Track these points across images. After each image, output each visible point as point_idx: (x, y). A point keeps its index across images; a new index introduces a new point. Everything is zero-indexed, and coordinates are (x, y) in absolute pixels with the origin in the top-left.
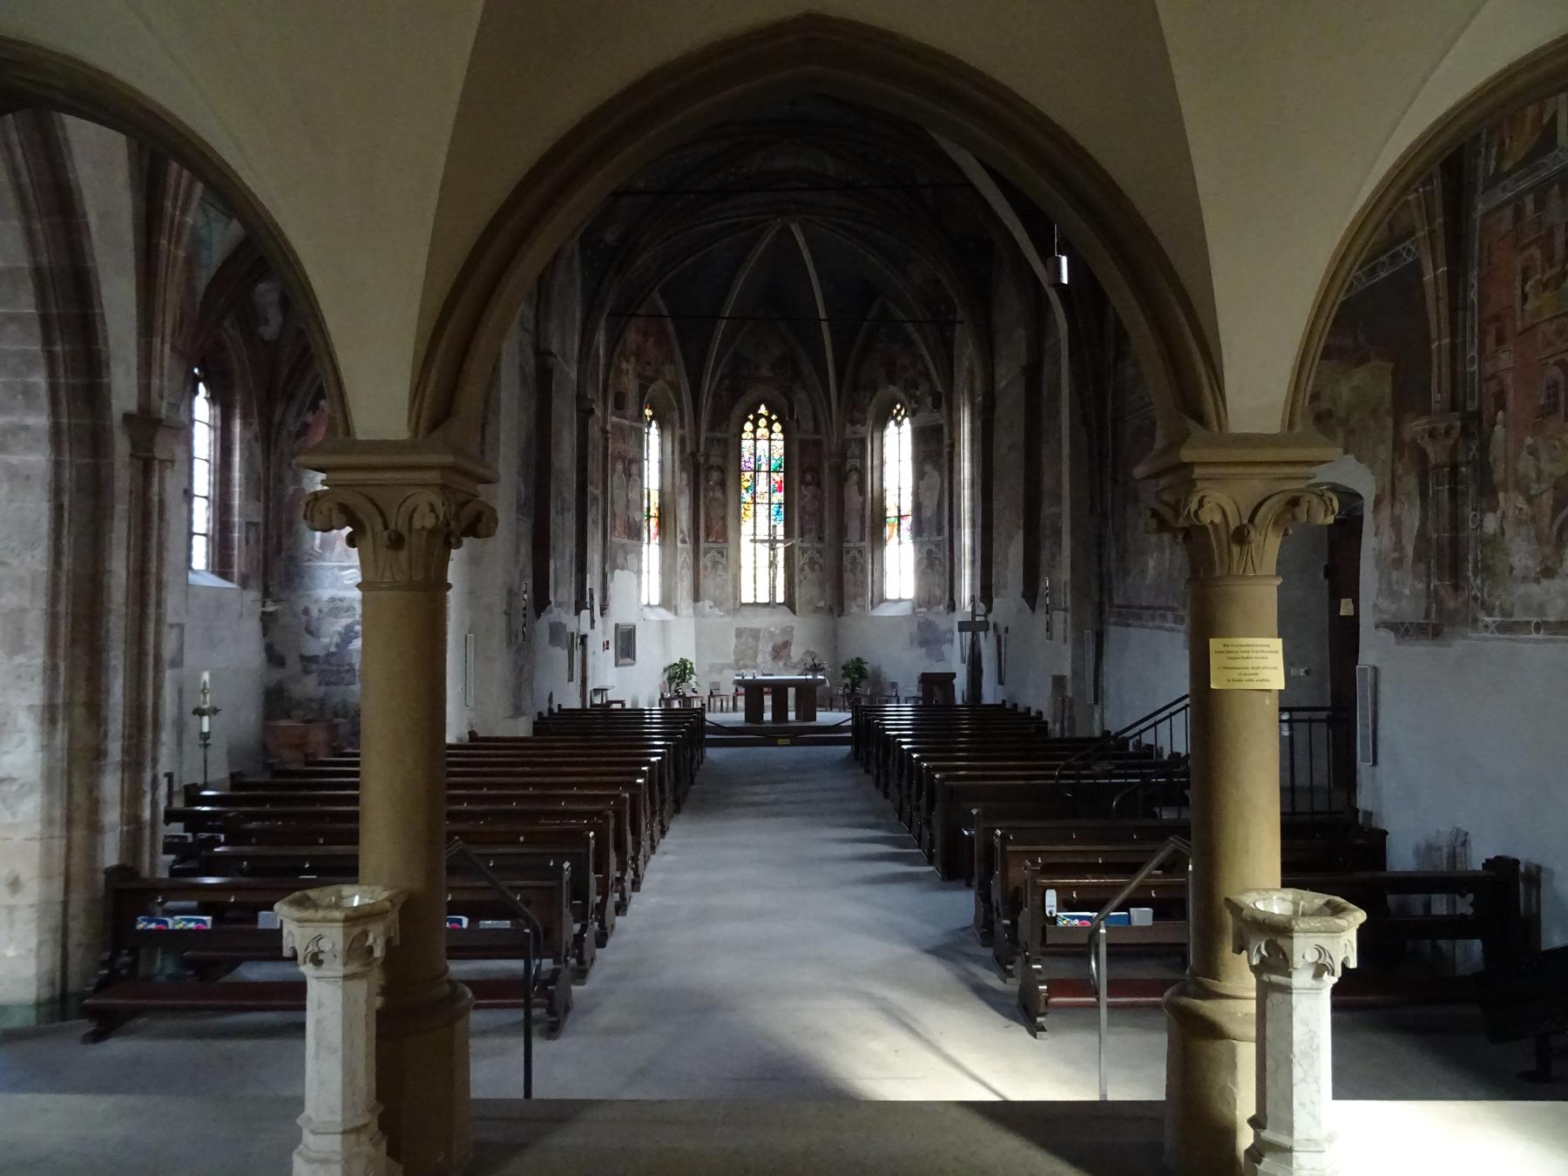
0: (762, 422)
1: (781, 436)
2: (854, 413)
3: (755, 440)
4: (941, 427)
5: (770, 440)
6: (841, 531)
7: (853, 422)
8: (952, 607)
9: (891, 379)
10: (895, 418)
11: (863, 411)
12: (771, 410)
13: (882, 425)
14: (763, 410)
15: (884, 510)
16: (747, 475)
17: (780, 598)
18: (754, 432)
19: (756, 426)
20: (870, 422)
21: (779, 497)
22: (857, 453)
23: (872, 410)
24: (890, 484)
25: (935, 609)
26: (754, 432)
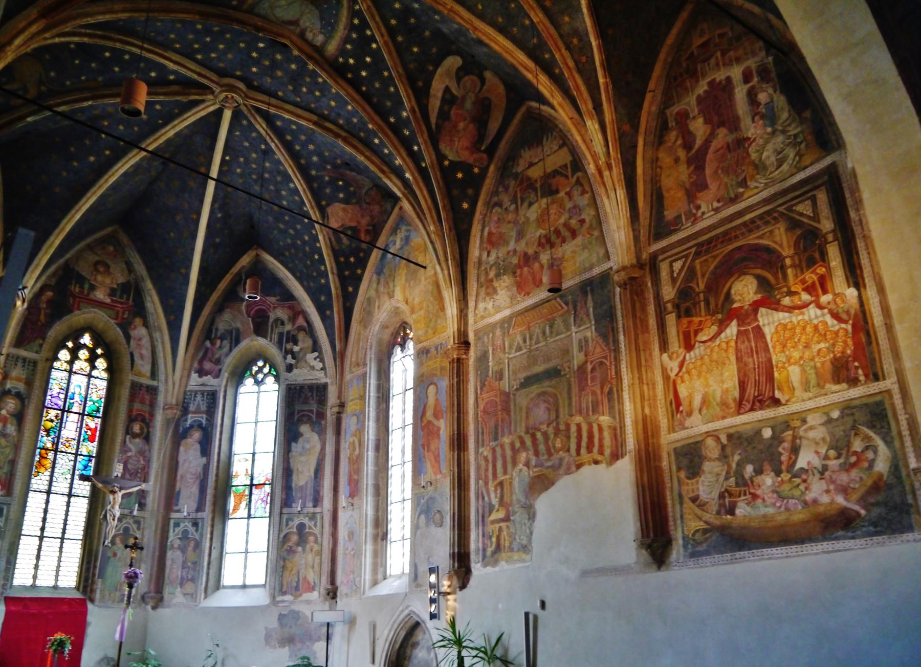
0: (83, 354)
1: (105, 375)
2: (204, 359)
3: (71, 372)
4: (325, 386)
5: (89, 376)
6: (171, 498)
7: (201, 373)
8: (332, 594)
9: (260, 329)
10: (254, 377)
11: (218, 362)
12: (98, 339)
13: (238, 377)
14: (86, 339)
15: (228, 476)
16: (52, 414)
17: (69, 579)
18: (71, 363)
19: (74, 357)
20: (225, 375)
21: (90, 448)
22: (204, 408)
23: (229, 362)
24: (242, 444)
25: (306, 596)
26: (71, 363)
